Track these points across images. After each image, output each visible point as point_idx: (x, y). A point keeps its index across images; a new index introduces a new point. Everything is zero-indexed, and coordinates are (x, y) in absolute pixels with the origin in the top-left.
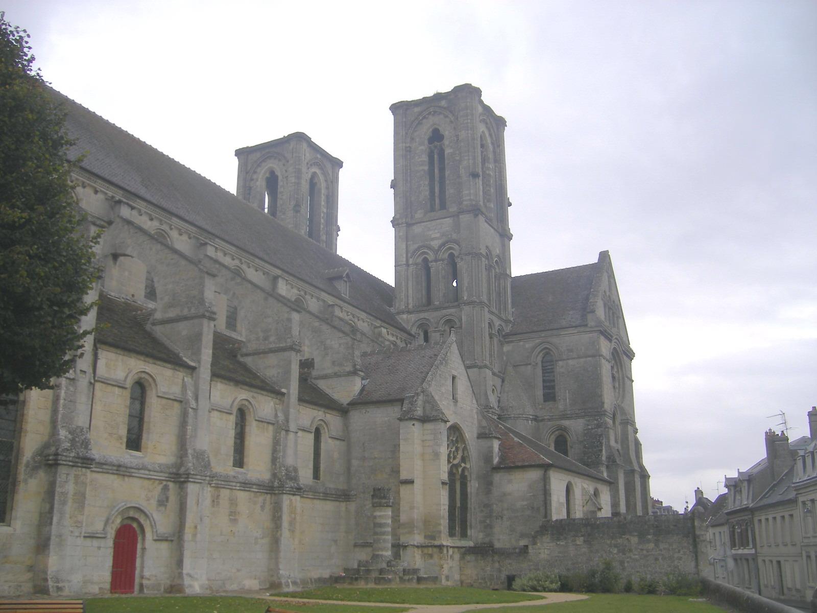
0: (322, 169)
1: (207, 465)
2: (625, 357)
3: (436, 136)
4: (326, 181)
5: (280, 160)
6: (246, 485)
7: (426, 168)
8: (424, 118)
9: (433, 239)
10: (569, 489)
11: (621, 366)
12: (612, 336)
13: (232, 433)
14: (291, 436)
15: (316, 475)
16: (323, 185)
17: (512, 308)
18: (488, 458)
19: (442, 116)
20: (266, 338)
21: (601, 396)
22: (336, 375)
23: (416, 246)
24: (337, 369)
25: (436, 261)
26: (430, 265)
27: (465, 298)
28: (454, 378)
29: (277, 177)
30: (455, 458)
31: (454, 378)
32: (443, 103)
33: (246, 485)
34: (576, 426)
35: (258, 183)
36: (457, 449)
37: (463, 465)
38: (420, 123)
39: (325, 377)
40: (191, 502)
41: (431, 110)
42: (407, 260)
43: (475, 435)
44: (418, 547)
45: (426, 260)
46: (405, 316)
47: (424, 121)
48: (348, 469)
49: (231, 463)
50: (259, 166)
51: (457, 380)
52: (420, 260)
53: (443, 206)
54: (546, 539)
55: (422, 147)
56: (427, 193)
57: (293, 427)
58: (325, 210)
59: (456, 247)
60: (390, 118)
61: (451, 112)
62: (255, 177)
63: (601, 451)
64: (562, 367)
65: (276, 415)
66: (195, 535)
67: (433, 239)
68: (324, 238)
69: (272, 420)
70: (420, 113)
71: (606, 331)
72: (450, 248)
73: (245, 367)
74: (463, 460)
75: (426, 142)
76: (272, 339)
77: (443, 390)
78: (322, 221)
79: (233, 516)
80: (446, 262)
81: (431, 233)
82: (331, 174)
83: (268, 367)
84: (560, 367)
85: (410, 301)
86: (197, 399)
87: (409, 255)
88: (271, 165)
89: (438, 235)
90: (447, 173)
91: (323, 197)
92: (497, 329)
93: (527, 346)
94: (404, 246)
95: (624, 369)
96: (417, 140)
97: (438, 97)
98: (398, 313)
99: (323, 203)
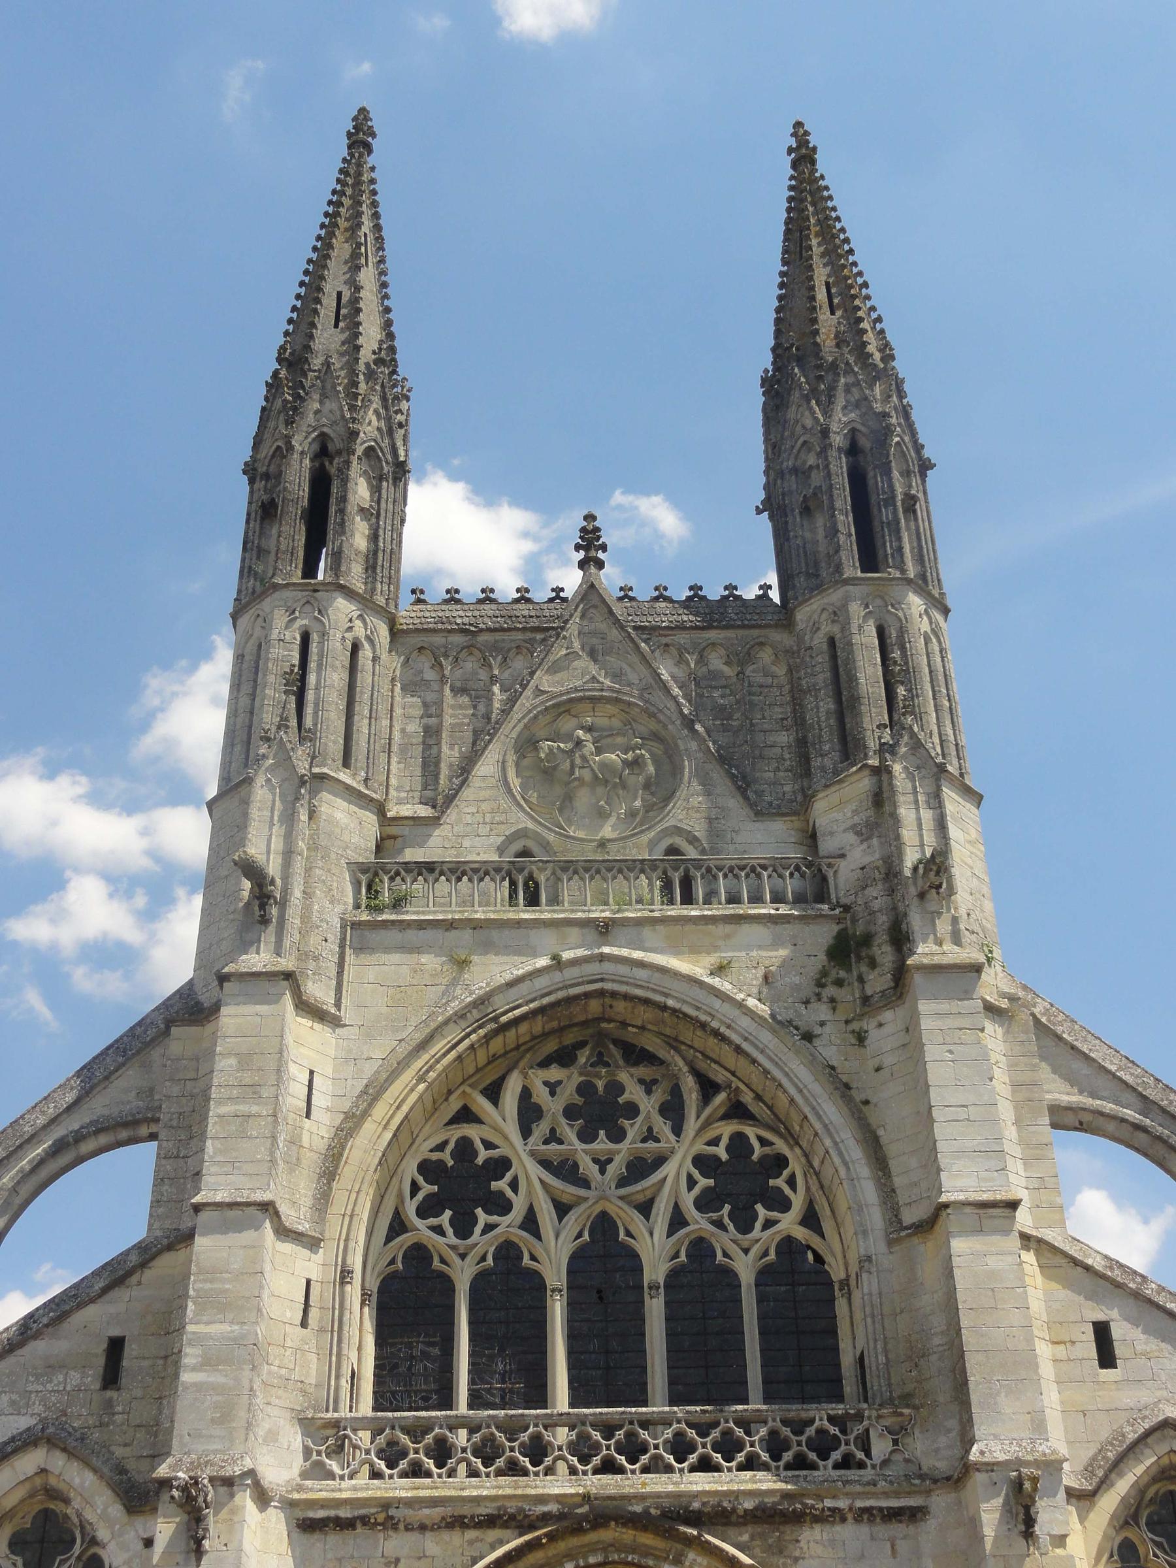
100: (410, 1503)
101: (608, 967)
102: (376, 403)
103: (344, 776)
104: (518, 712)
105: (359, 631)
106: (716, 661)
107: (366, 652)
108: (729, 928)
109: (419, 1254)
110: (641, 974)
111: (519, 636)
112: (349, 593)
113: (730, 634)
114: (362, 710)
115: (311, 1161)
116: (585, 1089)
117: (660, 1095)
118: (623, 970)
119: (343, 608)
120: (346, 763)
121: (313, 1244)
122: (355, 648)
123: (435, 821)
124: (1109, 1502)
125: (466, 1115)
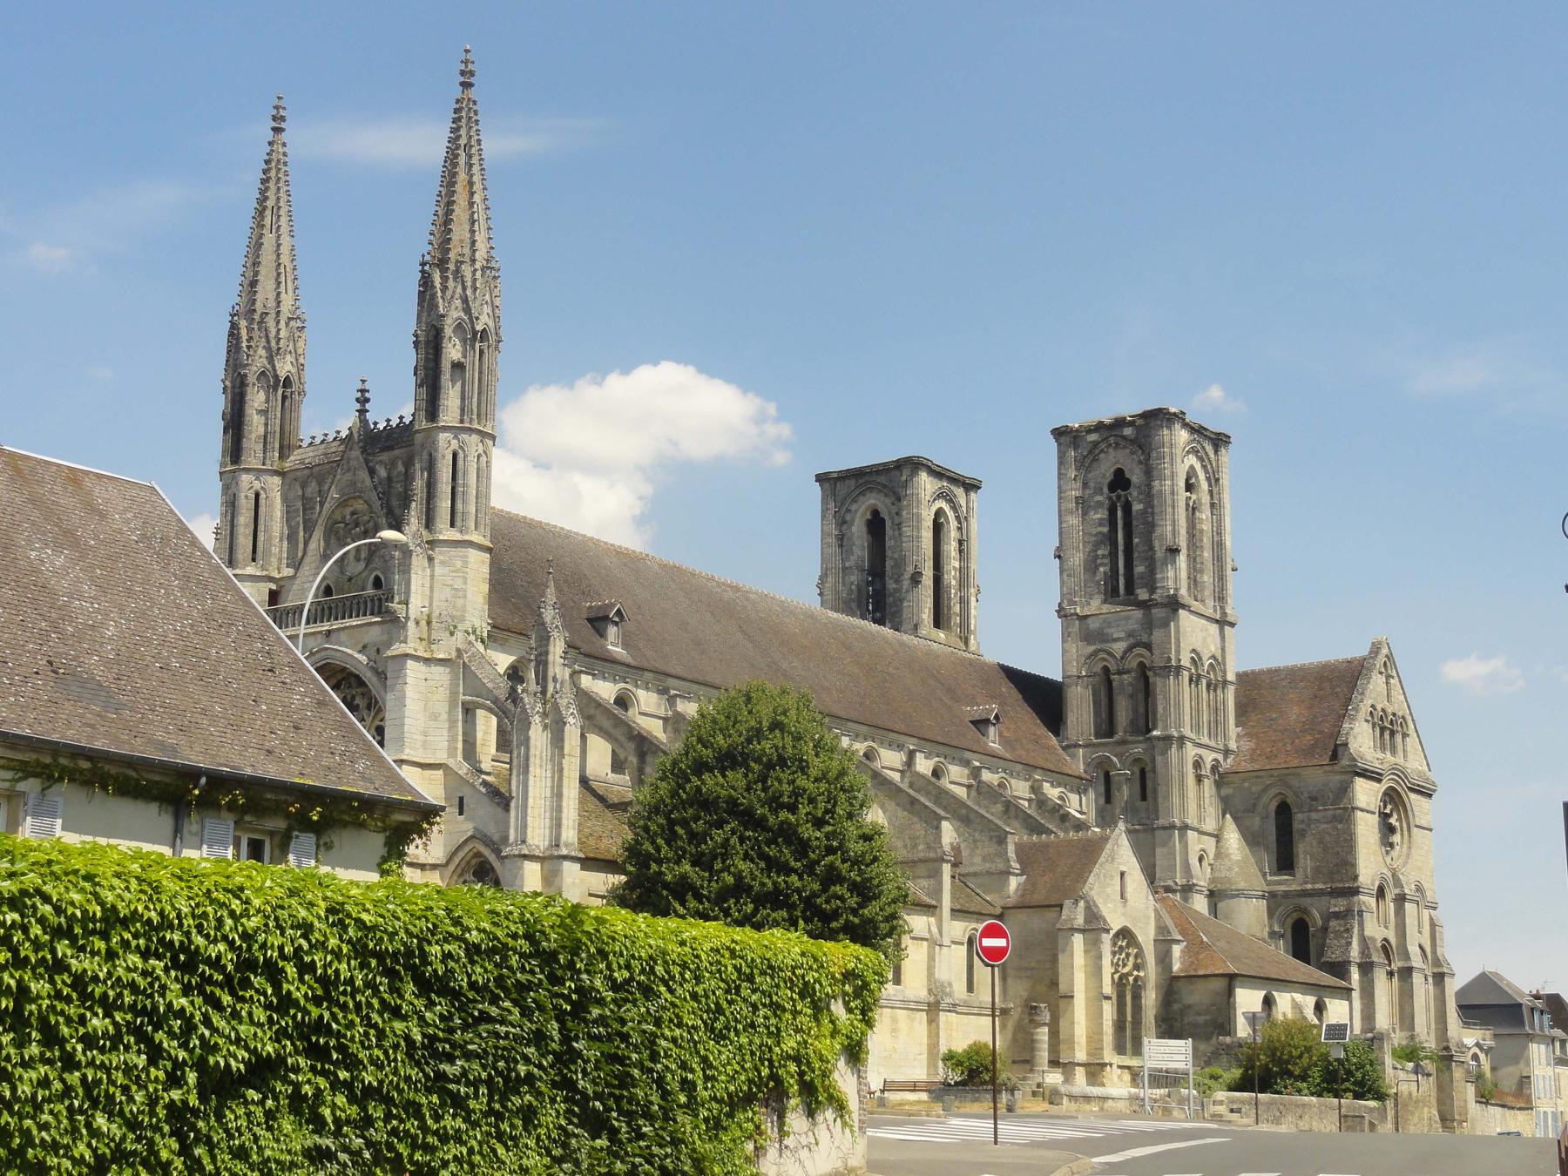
2: (1413, 796)
3: (1120, 481)
4: (958, 518)
5: (886, 495)
7: (1105, 529)
8: (1102, 451)
9: (1116, 640)
10: (1268, 1002)
11: (1406, 811)
12: (1381, 774)
15: (970, 988)
16: (953, 524)
19: (1127, 451)
20: (915, 846)
21: (1354, 865)
25: (1119, 673)
26: (1112, 677)
28: (1122, 874)
29: (883, 521)
30: (1124, 965)
31: (1122, 874)
32: (1128, 431)
35: (854, 529)
36: (1128, 955)
37: (1135, 973)
38: (1095, 460)
41: (1112, 440)
45: (1106, 670)
47: (1102, 455)
50: (854, 501)
51: (1128, 879)
52: (1098, 668)
53: (1130, 589)
55: (1099, 498)
56: (1108, 568)
57: (946, 941)
59: (1147, 653)
60: (1052, 445)
61: (1140, 447)
62: (848, 518)
63: (1349, 944)
64: (1303, 821)
65: (930, 931)
68: (957, 609)
69: (927, 935)
70: (1096, 444)
71: (1366, 770)
72: (1141, 656)
74: (1137, 967)
75: (1106, 490)
76: (921, 847)
77: (1109, 890)
78: (953, 582)
80: (1133, 674)
81: (1112, 630)
82: (964, 505)
88: (873, 501)
89: (1122, 635)
90: (1136, 540)
91: (954, 545)
92: (1209, 766)
93: (1254, 789)
95: (1410, 813)
96: (1092, 485)
97: (1120, 423)
99: (953, 554)
101: (328, 652)
102: (263, 342)
103: (250, 570)
104: (324, 513)
105: (257, 485)
106: (401, 468)
107: (263, 496)
108: (366, 628)
110: (339, 654)
111: (327, 466)
112: (247, 470)
113: (402, 451)
114: (261, 527)
117: (366, 701)
118: (333, 653)
119: (245, 478)
120: (254, 560)
122: (257, 495)
123: (294, 577)
124: (452, 867)
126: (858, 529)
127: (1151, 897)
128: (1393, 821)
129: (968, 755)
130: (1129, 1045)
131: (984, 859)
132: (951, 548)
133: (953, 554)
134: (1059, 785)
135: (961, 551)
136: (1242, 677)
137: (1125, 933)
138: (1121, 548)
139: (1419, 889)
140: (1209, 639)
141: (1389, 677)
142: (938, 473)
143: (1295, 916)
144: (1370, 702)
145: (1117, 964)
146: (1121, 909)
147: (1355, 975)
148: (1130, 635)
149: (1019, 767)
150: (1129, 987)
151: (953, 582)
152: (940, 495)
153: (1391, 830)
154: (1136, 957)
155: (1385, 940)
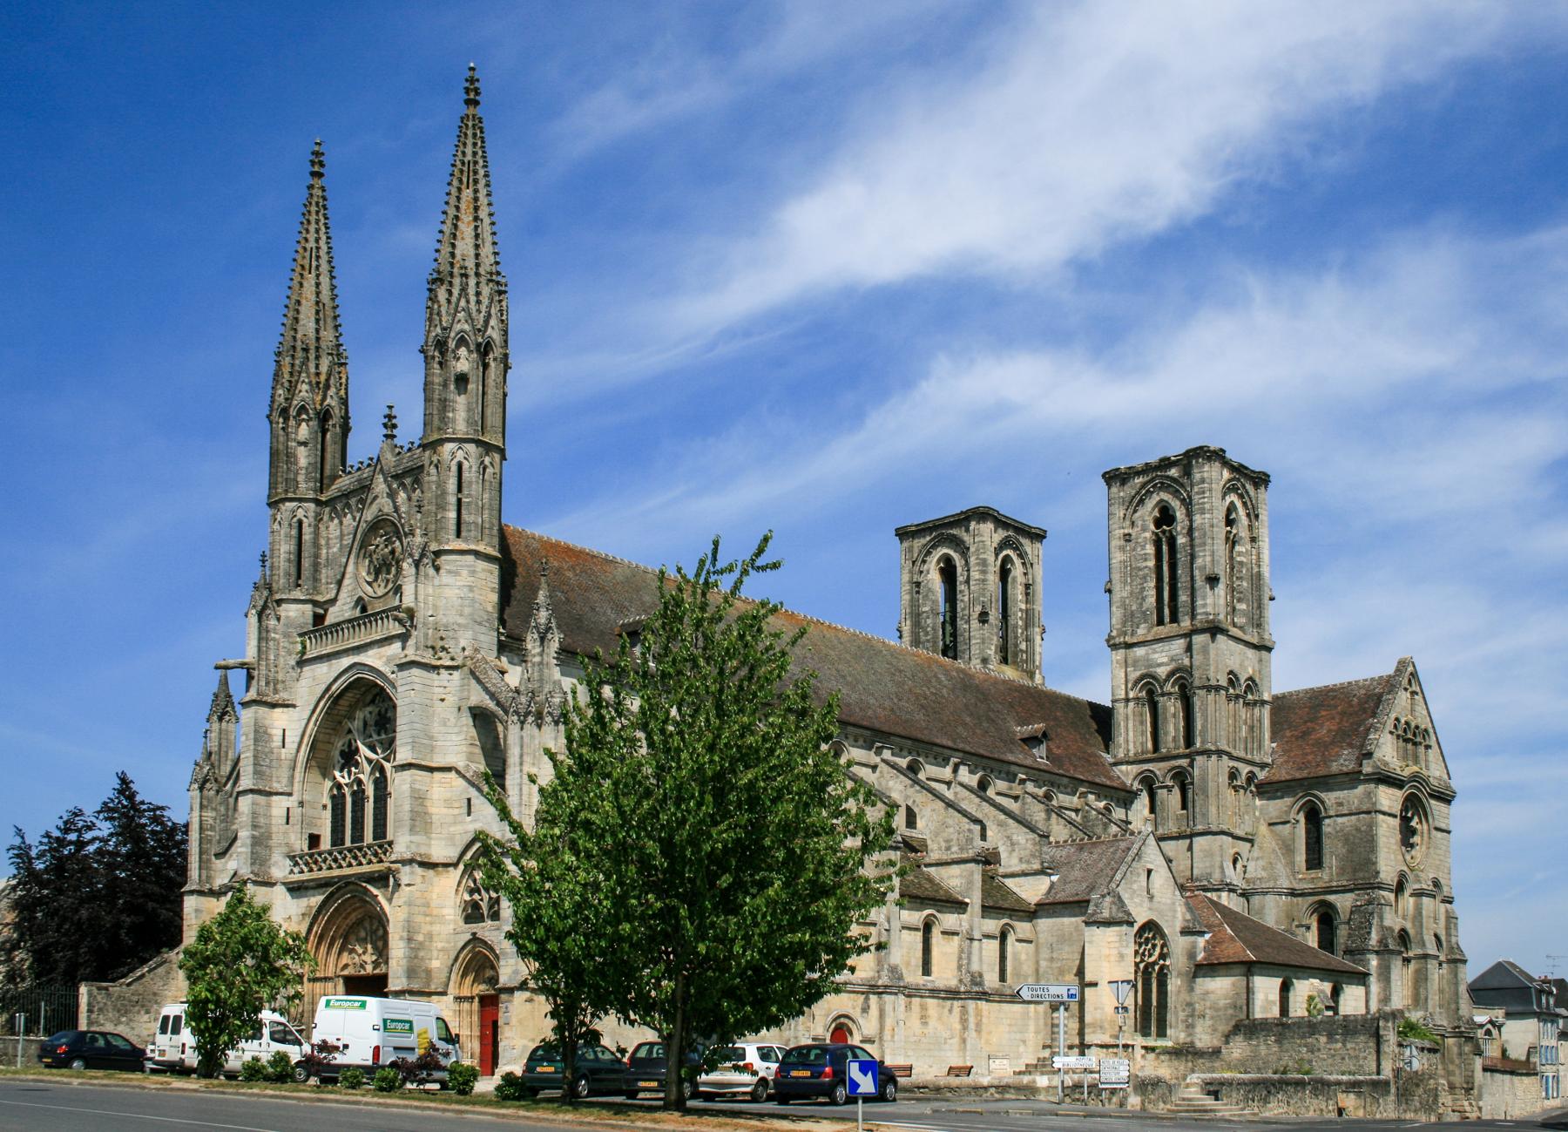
0: (1016, 549)
1: (901, 978)
6: (934, 993)
9: (1159, 665)
13: (920, 946)
14: (976, 943)
15: (1003, 978)
17: (1273, 740)
18: (1191, 955)
20: (948, 849)
21: (1375, 863)
22: (1024, 874)
23: (1138, 674)
24: (1024, 867)
27: (1198, 745)
28: (1149, 872)
30: (1150, 955)
33: (934, 993)
34: (1343, 903)
36: (1154, 946)
37: (1161, 962)
39: (1013, 875)
40: (889, 1008)
42: (1127, 693)
43: (1178, 929)
44: (1102, 1046)
46: (1124, 768)
48: (1037, 971)
49: (920, 973)
54: (1239, 1039)
58: (1023, 606)
63: (1369, 933)
66: (893, 1036)
67: (1159, 665)
68: (1023, 646)
73: (930, 880)
74: (1163, 956)
76: (955, 849)
77: (1135, 886)
78: (1020, 623)
79: (924, 1019)
81: (1156, 656)
83: (953, 879)
84: (1328, 826)
85: (1131, 746)
86: (889, 922)
87: (1130, 686)
89: (1165, 660)
94: (1123, 675)
98: (1115, 764)
100: (308, 881)
109: (339, 786)
115: (286, 764)
116: (379, 713)
121: (290, 794)
125: (350, 731)
126: (934, 579)
127: (1177, 893)
128: (1413, 824)
129: (1014, 768)
130: (1153, 1029)
131: (1021, 859)
132: (1017, 593)
133: (1020, 597)
134: (1106, 797)
135: (1027, 594)
136: (1276, 698)
137: (1151, 926)
138: (1166, 579)
139: (1436, 884)
140: (1246, 663)
141: (1414, 693)
142: (1001, 522)
143: (1322, 910)
144: (1393, 716)
145: (1143, 954)
146: (1146, 904)
147: (1374, 962)
148: (1172, 660)
149: (1065, 781)
150: (1154, 975)
151: (1020, 623)
152: (1005, 544)
153: (1413, 832)
154: (1162, 947)
155: (1403, 930)
